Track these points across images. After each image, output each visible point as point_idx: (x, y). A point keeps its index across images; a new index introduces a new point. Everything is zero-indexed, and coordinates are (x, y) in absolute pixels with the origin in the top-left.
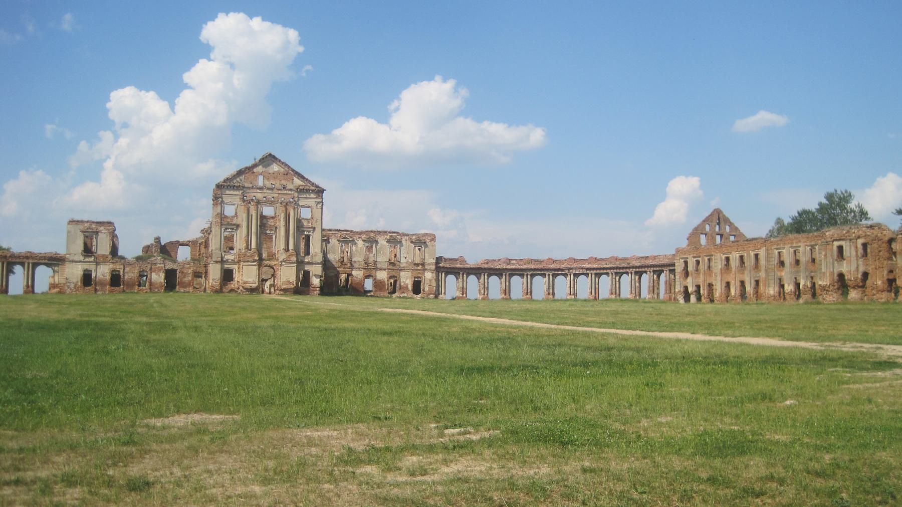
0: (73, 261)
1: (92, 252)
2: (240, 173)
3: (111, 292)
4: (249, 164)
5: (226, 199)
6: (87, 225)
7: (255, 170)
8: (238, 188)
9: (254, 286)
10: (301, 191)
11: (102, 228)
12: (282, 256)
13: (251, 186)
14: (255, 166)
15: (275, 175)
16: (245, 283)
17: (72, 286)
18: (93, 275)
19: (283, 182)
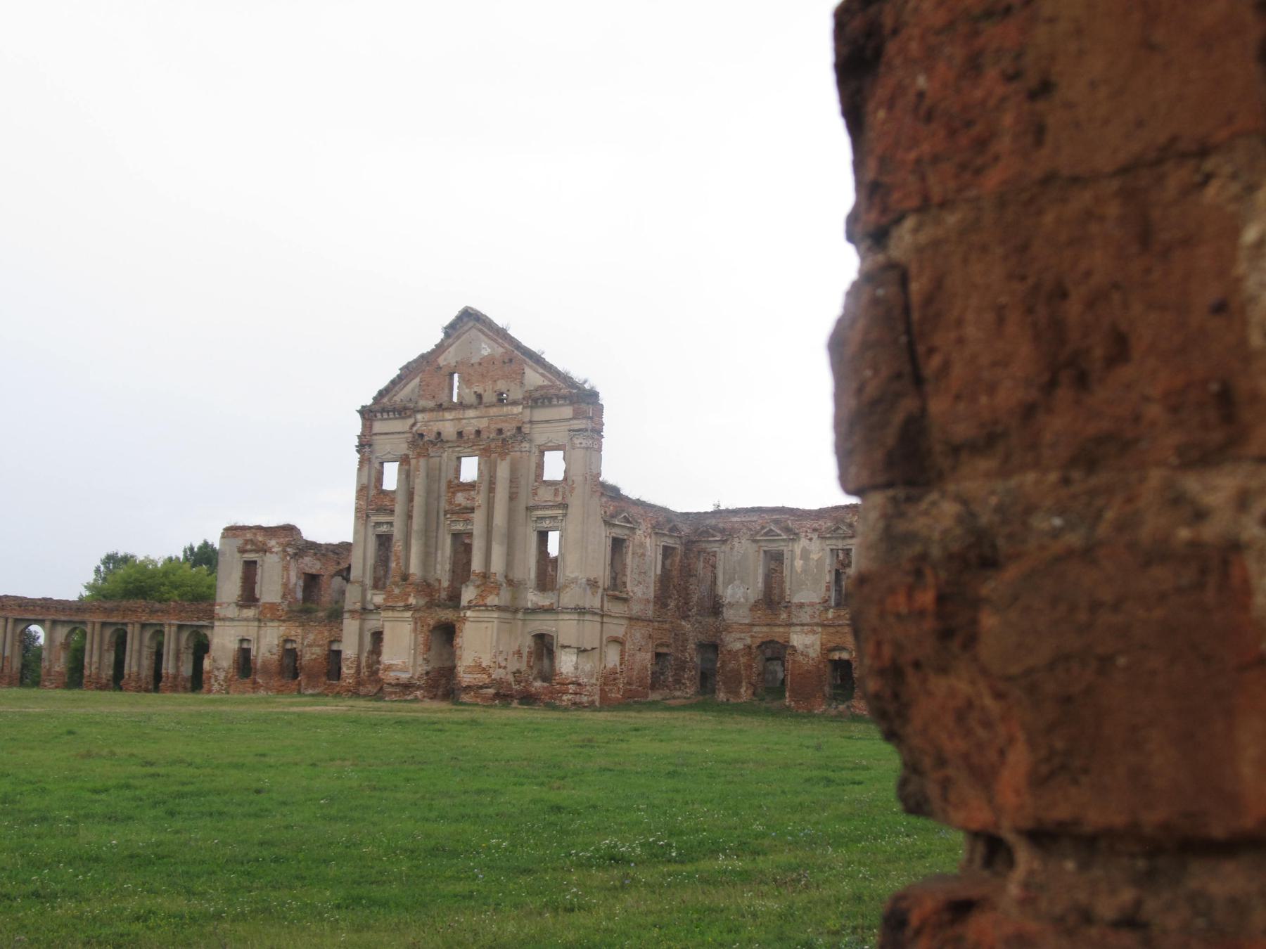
0: (224, 619)
1: (257, 600)
2: (408, 372)
3: (279, 692)
4: (428, 346)
5: (382, 446)
6: (249, 536)
7: (441, 361)
8: (402, 412)
9: (404, 677)
10: (538, 399)
11: (273, 543)
12: (468, 594)
13: (431, 404)
14: (440, 348)
15: (484, 369)
16: (389, 668)
17: (222, 676)
18: (253, 652)
19: (501, 385)
